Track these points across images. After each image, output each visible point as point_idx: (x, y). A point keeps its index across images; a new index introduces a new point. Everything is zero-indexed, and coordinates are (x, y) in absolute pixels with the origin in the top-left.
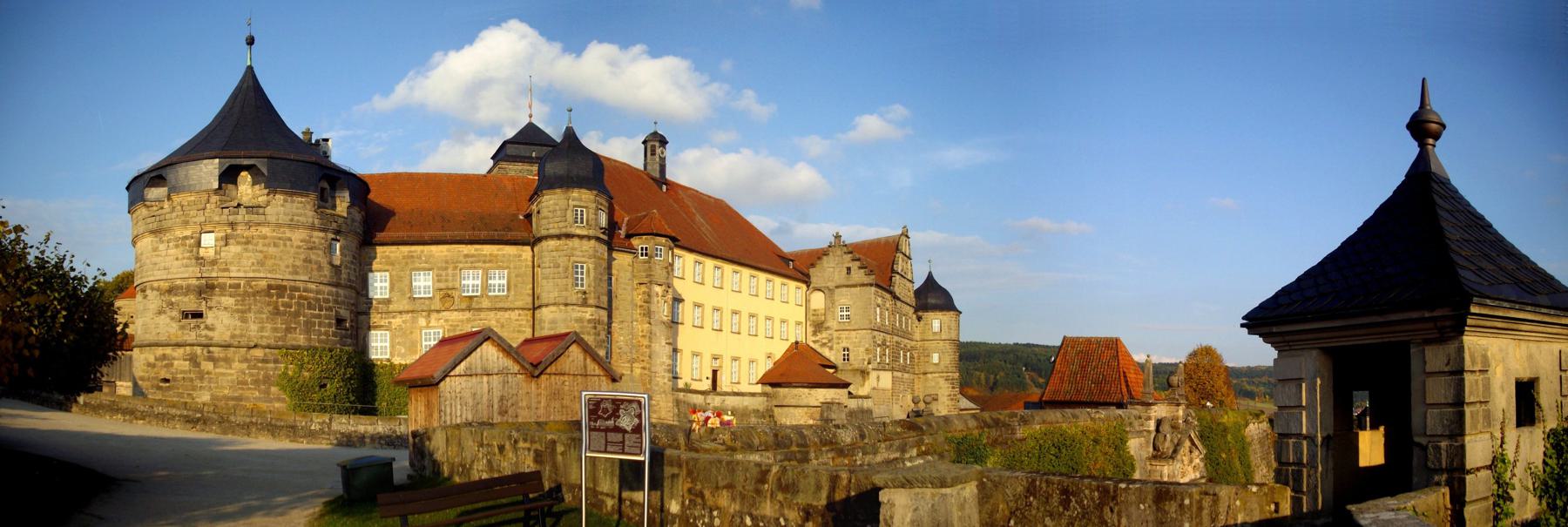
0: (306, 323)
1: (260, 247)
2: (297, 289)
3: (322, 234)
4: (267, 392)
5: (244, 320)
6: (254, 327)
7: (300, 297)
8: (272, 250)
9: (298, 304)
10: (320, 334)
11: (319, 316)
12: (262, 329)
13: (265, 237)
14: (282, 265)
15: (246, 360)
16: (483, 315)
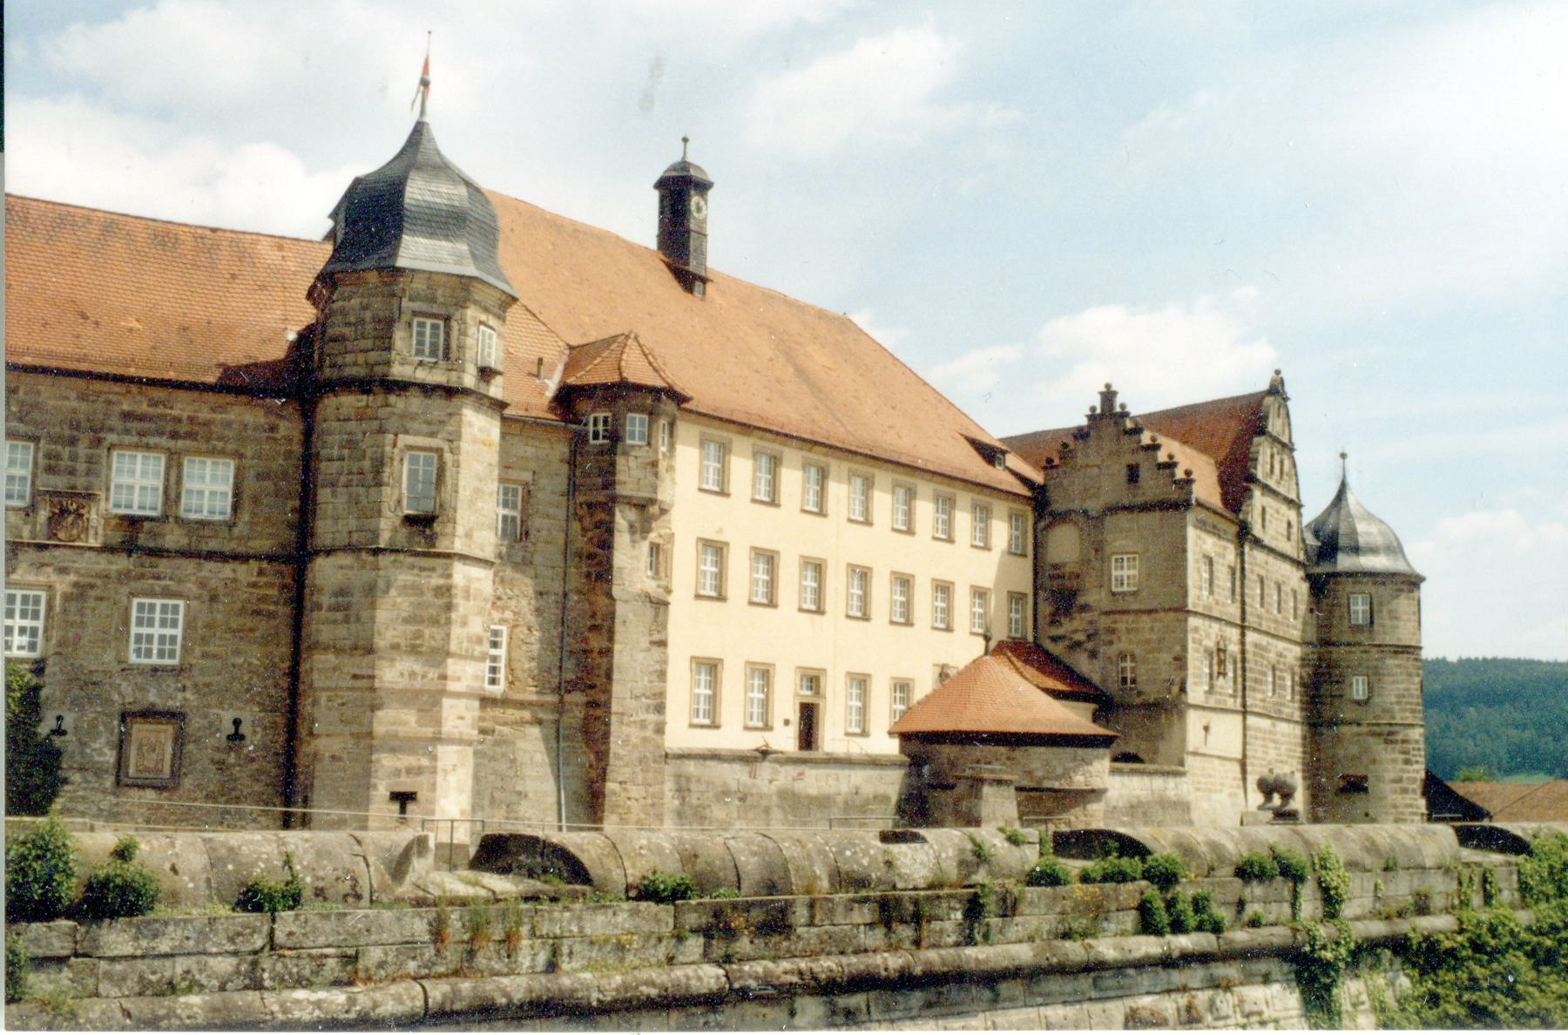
16: (164, 566)
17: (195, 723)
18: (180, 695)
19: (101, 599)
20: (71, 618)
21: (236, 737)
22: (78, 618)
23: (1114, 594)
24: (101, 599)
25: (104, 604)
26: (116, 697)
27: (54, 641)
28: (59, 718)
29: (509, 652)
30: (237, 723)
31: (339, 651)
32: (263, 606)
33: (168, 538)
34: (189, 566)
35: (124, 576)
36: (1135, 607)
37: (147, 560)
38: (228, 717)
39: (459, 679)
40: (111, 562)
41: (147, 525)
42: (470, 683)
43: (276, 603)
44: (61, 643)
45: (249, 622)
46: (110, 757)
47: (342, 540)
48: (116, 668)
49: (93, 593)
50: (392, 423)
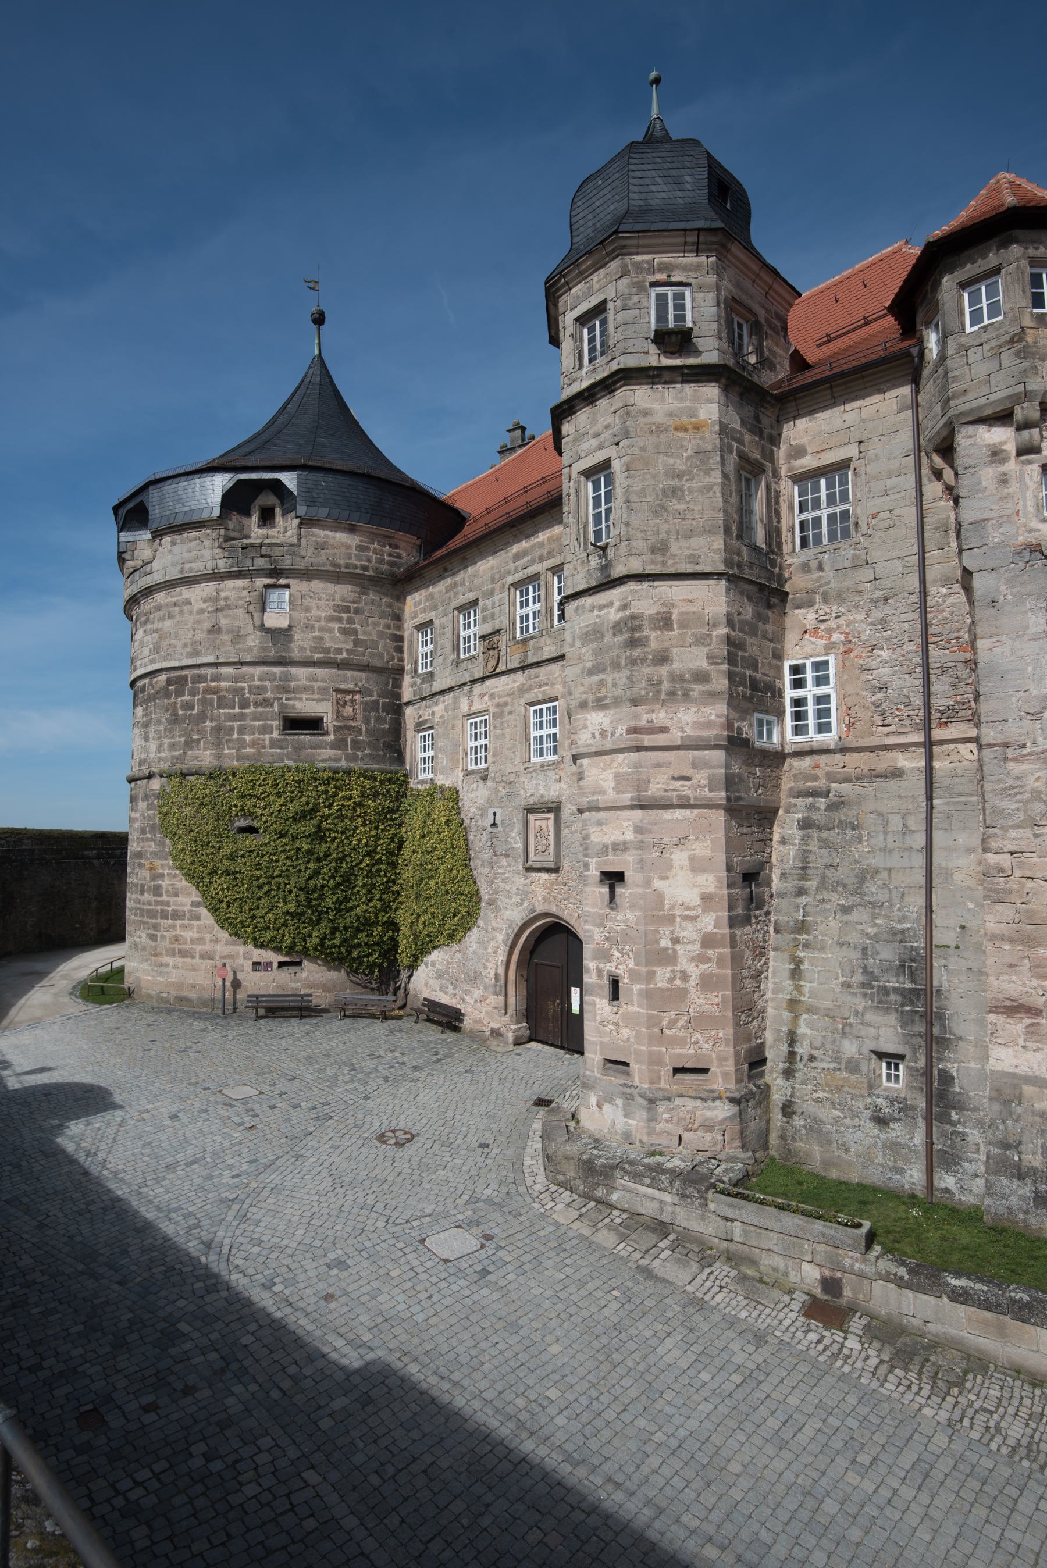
0: (218, 730)
1: (157, 625)
2: (201, 679)
3: (240, 583)
4: (162, 844)
5: (147, 740)
6: (153, 746)
7: (207, 690)
8: (168, 624)
9: (204, 702)
10: (242, 744)
11: (242, 717)
12: (160, 747)
13: (159, 608)
14: (178, 644)
15: (146, 797)
16: (542, 671)
17: (568, 810)
18: (558, 785)
19: (510, 713)
24: (510, 713)
26: (522, 792)
29: (841, 686)
35: (522, 691)
37: (533, 671)
39: (664, 730)
40: (514, 681)
42: (689, 731)
49: (507, 709)
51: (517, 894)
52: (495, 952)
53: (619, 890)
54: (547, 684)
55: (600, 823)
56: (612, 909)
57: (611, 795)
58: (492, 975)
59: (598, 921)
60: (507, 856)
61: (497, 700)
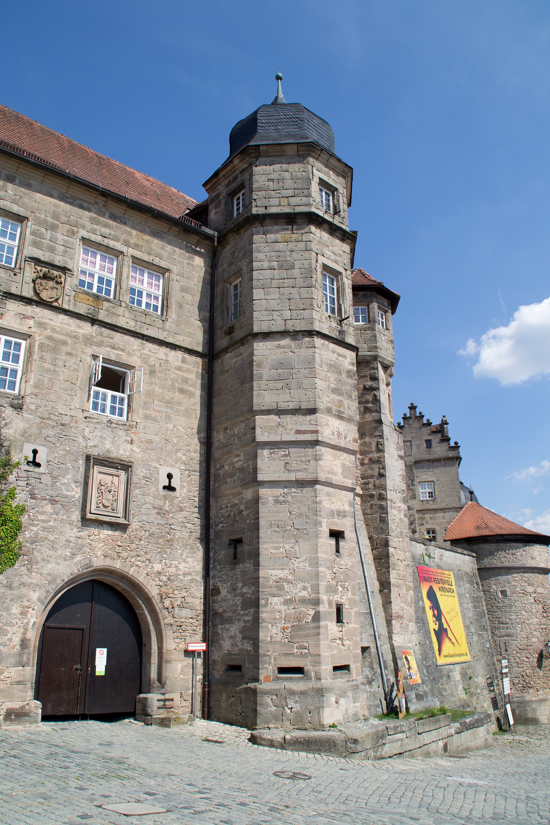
16: (118, 337)
19: (69, 354)
20: (46, 365)
21: (169, 488)
22: (52, 368)
23: (422, 501)
24: (69, 354)
25: (72, 361)
27: (31, 383)
28: (35, 452)
30: (170, 476)
31: (279, 412)
32: (186, 387)
33: (121, 318)
34: (135, 343)
35: (88, 341)
36: (434, 507)
37: (106, 331)
38: (163, 472)
40: (79, 327)
41: (106, 304)
43: (194, 386)
44: (36, 386)
45: (177, 396)
46: (77, 493)
47: (279, 326)
48: (81, 415)
49: (65, 349)
50: (314, 246)
51: (66, 547)
52: (24, 613)
53: (342, 543)
54: (123, 350)
55: (328, 495)
56: (338, 556)
57: (338, 479)
58: (16, 640)
59: (329, 565)
60: (53, 501)
61: (48, 332)
